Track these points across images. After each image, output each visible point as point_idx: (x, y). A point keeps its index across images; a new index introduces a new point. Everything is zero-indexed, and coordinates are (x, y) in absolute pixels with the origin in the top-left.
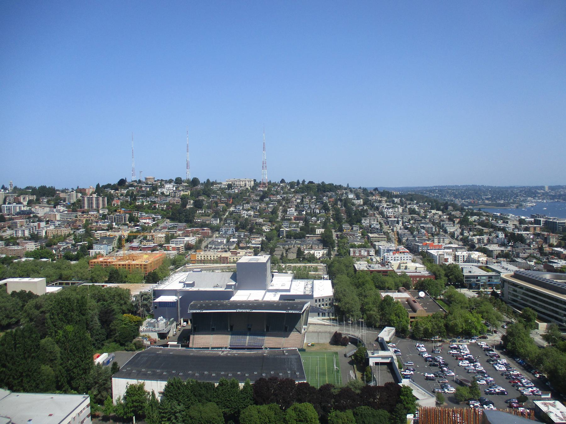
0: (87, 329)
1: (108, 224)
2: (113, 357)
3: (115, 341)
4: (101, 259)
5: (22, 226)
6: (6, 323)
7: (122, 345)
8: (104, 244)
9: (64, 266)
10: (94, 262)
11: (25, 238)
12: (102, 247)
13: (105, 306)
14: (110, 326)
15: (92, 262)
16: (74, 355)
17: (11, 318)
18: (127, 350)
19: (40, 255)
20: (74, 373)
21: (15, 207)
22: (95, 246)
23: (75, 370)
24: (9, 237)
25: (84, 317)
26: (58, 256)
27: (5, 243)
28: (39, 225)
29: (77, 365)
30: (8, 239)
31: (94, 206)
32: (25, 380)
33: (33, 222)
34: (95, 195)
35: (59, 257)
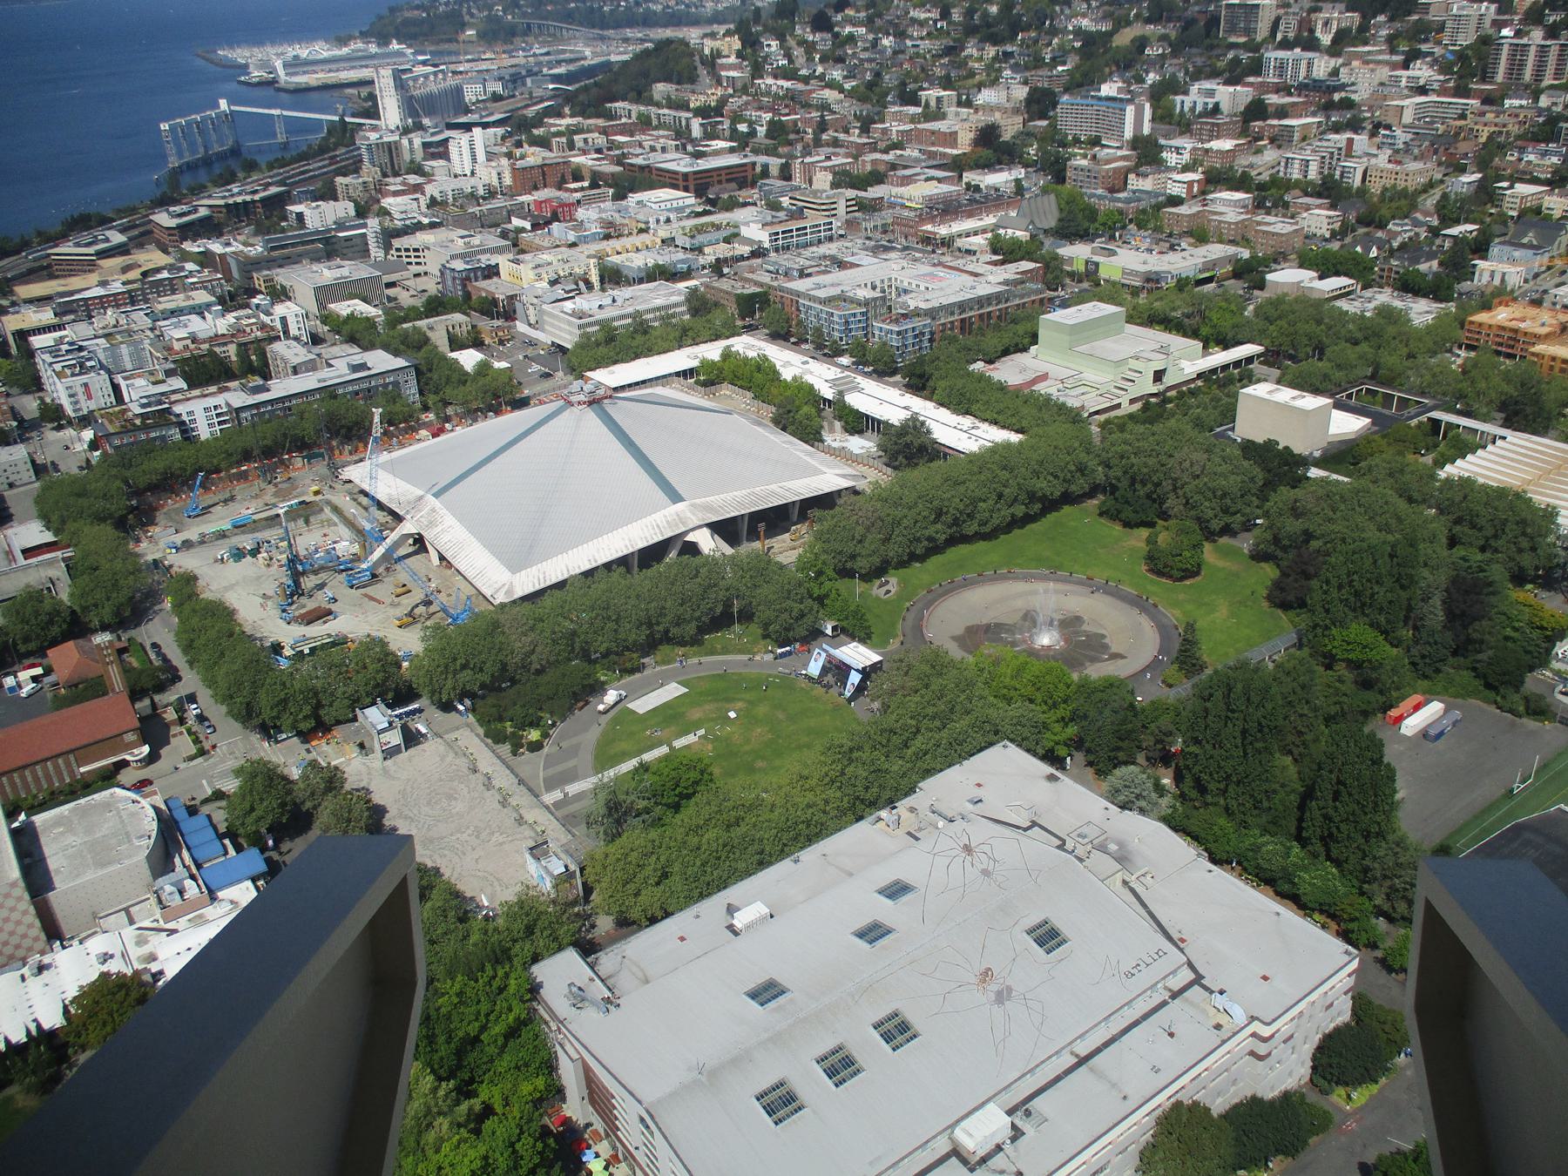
0: (1407, 619)
1: (1555, 160)
2: (1454, 724)
3: (1474, 669)
4: (1501, 316)
5: (1304, 139)
6: (1222, 523)
7: (1488, 686)
8: (1524, 246)
9: (1391, 330)
10: (1480, 325)
11: (1308, 189)
12: (1517, 254)
13: (1470, 567)
14: (1470, 631)
15: (1472, 323)
16: (1350, 795)
17: (1235, 513)
18: (1498, 708)
19: (1334, 265)
20: (1339, 831)
21: (1297, 61)
22: (1495, 250)
23: (1343, 826)
24: (1265, 177)
25: (1404, 595)
26: (1382, 270)
27: (1254, 199)
28: (1351, 141)
29: (1351, 818)
30: (1262, 187)
31: (1528, 75)
32: (1230, 789)
33: (1337, 129)
34: (1537, 36)
35: (1385, 274)
